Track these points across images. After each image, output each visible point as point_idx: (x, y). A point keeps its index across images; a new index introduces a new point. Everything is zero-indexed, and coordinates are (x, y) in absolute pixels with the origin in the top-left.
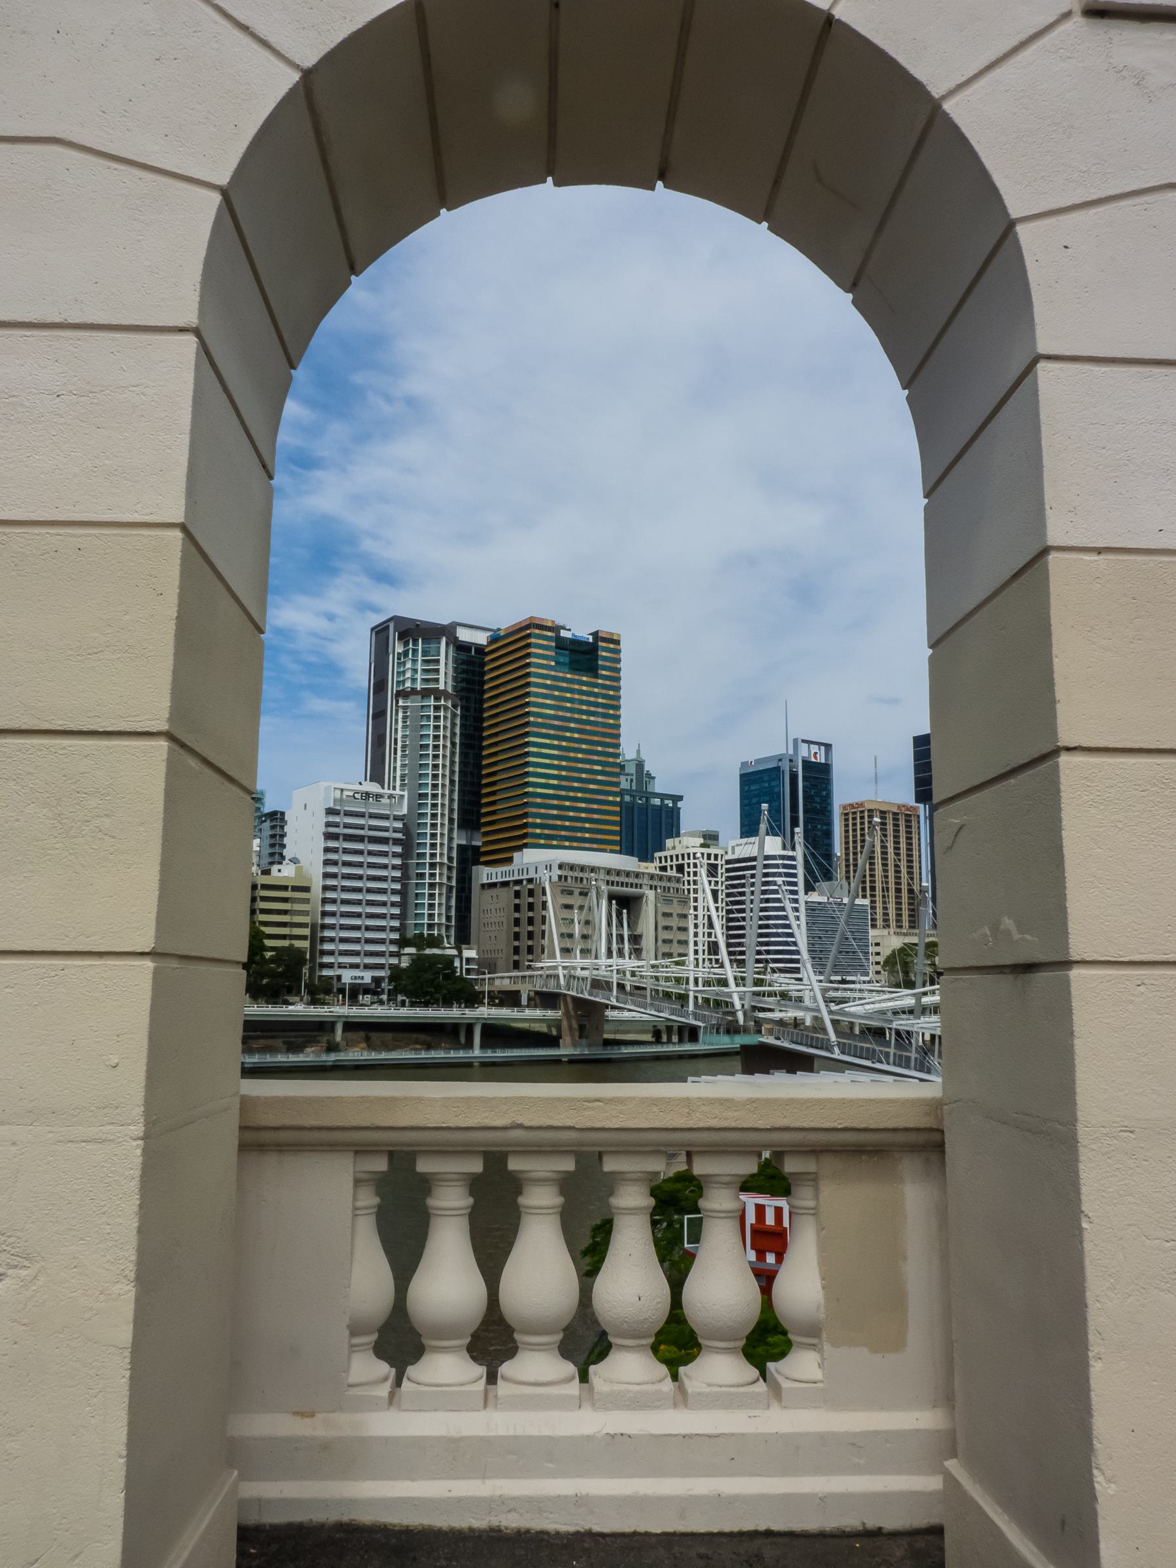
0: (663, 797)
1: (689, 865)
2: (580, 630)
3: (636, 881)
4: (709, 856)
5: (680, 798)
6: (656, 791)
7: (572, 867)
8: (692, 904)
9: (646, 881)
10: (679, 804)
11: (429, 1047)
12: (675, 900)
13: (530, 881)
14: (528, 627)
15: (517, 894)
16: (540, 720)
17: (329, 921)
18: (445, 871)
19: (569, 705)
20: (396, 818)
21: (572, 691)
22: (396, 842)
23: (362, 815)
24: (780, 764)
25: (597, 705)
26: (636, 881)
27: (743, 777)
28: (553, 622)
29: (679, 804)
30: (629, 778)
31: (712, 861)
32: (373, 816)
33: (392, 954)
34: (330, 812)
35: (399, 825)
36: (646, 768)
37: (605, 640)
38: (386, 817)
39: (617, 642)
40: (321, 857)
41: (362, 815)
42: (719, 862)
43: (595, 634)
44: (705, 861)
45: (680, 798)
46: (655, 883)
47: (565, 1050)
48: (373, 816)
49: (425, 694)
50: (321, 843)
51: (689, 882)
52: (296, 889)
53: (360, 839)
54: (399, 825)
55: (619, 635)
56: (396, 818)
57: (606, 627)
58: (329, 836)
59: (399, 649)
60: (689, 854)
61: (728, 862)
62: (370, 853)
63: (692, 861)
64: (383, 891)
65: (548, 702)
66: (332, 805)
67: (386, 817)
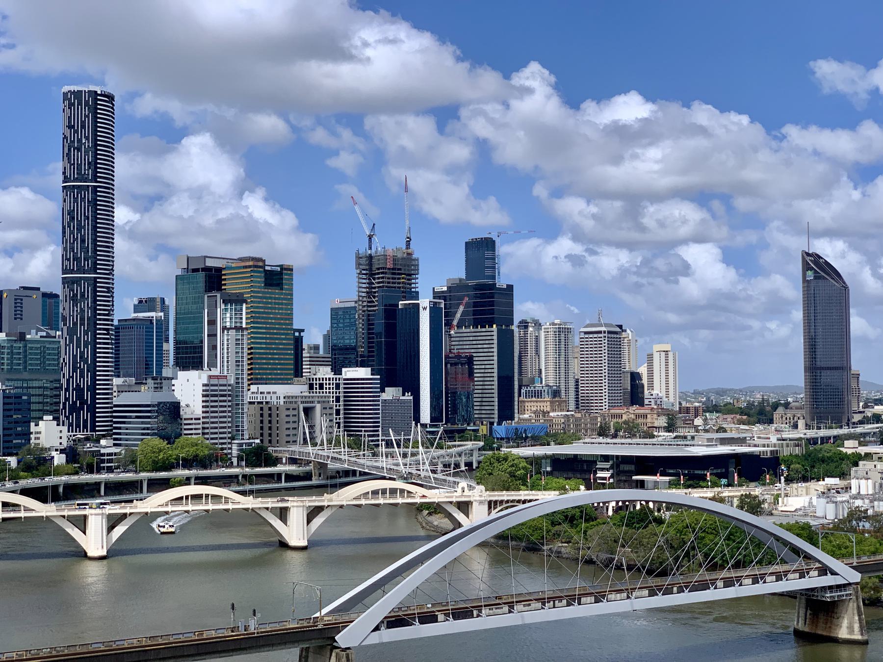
2: (273, 261)
5: (303, 331)
7: (289, 397)
10: (302, 334)
11: (268, 483)
13: (267, 403)
15: (262, 409)
17: (206, 431)
21: (271, 298)
23: (216, 385)
25: (282, 304)
29: (302, 334)
32: (221, 385)
33: (230, 443)
34: (204, 385)
35: (230, 388)
37: (286, 269)
39: (292, 270)
40: (201, 404)
41: (216, 385)
43: (281, 266)
45: (303, 331)
46: (320, 399)
47: (315, 481)
48: (221, 385)
49: (236, 328)
50: (201, 399)
52: (196, 419)
53: (216, 396)
54: (230, 388)
56: (229, 385)
57: (286, 262)
58: (203, 396)
59: (223, 307)
61: (345, 380)
62: (221, 401)
64: (225, 417)
66: (206, 382)
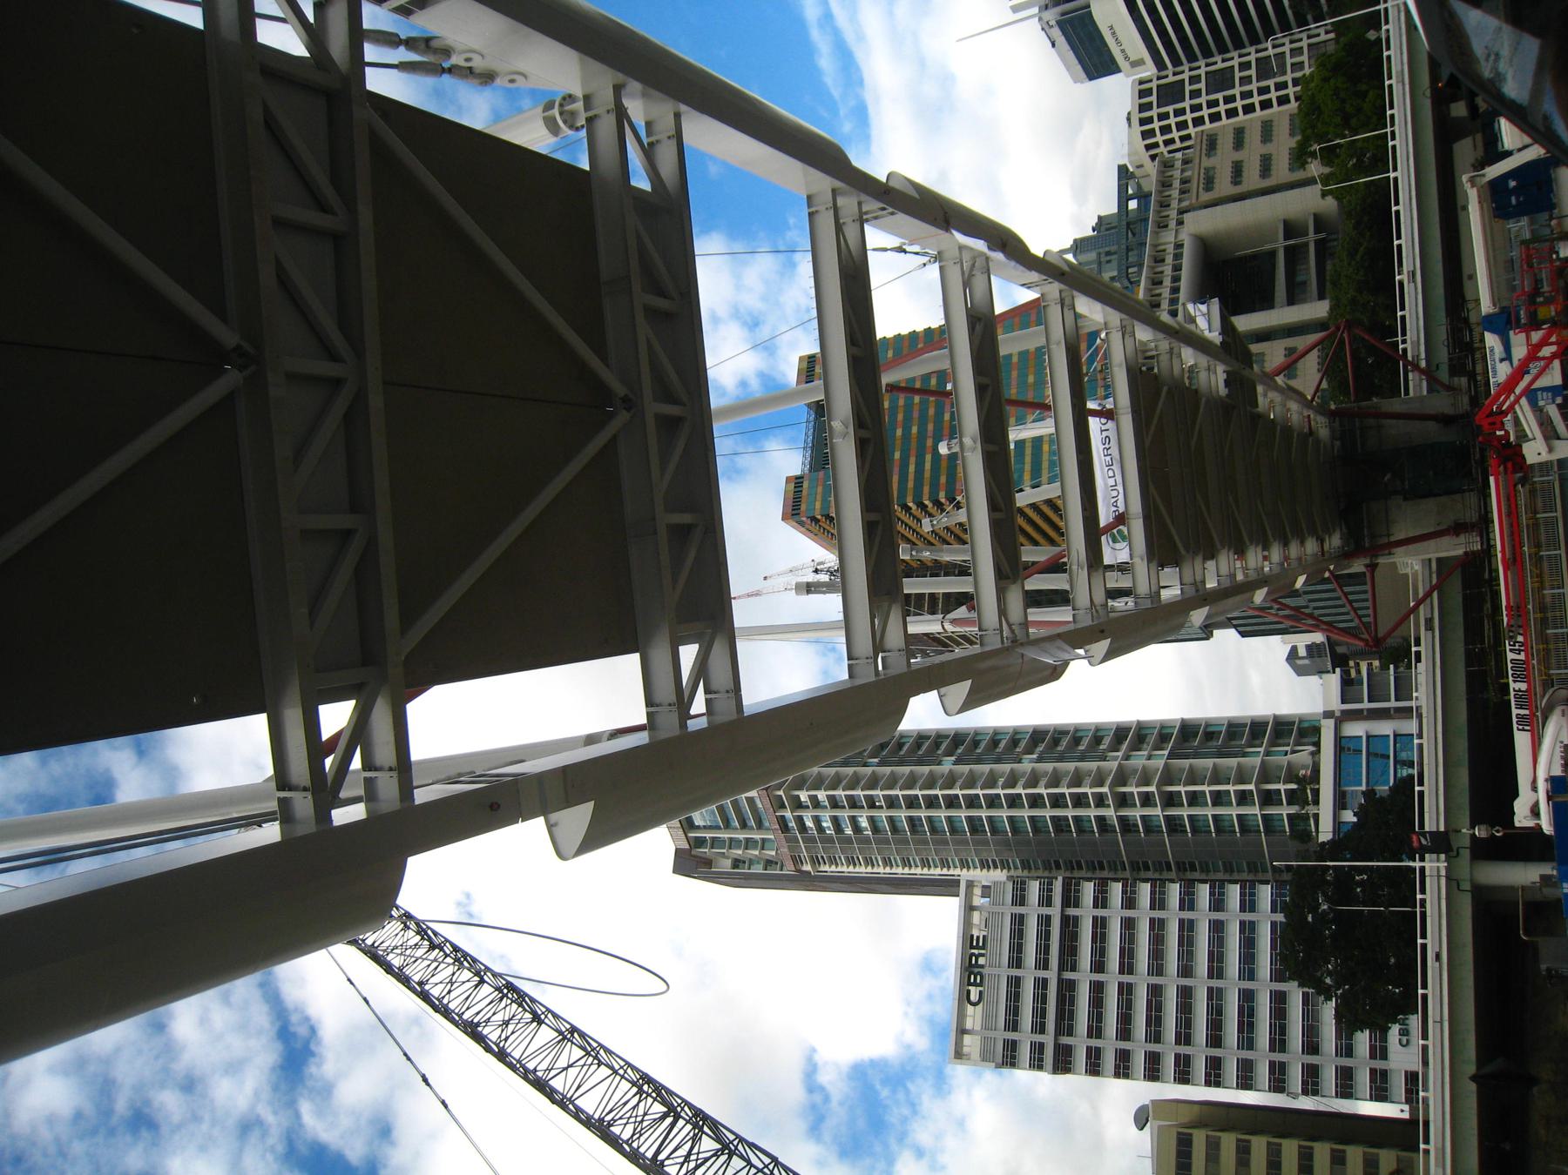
0: (1123, 199)
1: (1166, 143)
3: (1169, 259)
4: (1148, 107)
6: (1115, 210)
8: (1208, 125)
9: (1168, 238)
12: (1206, 163)
14: (802, 524)
16: (943, 479)
18: (1139, 760)
19: (915, 430)
20: (1020, 899)
22: (1071, 899)
23: (1015, 983)
24: (1053, 23)
26: (1169, 259)
27: (1091, 78)
28: (788, 479)
30: (1104, 259)
31: (1154, 99)
32: (1017, 961)
36: (1090, 233)
38: (1019, 921)
41: (1015, 983)
42: (1154, 85)
44: (1154, 113)
48: (1017, 961)
51: (1167, 143)
53: (1067, 990)
55: (801, 358)
56: (1020, 899)
60: (1148, 147)
63: (1159, 139)
65: (912, 468)
67: (1019, 921)
